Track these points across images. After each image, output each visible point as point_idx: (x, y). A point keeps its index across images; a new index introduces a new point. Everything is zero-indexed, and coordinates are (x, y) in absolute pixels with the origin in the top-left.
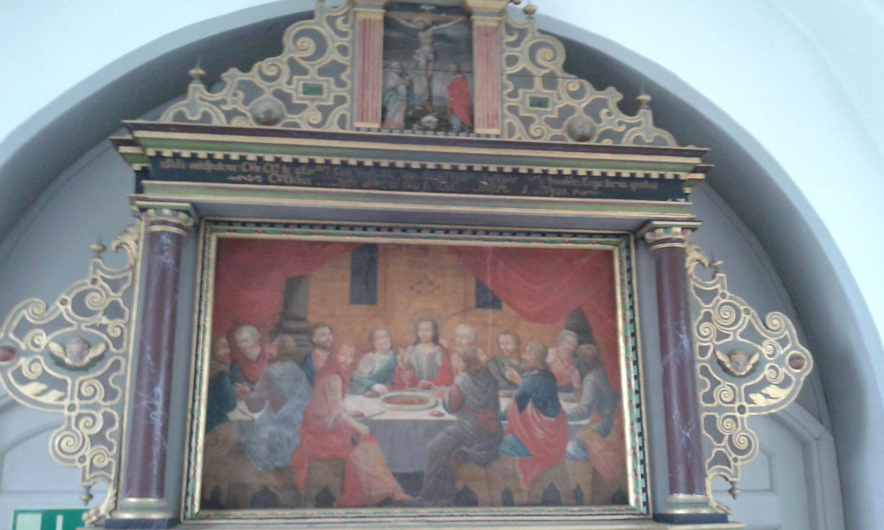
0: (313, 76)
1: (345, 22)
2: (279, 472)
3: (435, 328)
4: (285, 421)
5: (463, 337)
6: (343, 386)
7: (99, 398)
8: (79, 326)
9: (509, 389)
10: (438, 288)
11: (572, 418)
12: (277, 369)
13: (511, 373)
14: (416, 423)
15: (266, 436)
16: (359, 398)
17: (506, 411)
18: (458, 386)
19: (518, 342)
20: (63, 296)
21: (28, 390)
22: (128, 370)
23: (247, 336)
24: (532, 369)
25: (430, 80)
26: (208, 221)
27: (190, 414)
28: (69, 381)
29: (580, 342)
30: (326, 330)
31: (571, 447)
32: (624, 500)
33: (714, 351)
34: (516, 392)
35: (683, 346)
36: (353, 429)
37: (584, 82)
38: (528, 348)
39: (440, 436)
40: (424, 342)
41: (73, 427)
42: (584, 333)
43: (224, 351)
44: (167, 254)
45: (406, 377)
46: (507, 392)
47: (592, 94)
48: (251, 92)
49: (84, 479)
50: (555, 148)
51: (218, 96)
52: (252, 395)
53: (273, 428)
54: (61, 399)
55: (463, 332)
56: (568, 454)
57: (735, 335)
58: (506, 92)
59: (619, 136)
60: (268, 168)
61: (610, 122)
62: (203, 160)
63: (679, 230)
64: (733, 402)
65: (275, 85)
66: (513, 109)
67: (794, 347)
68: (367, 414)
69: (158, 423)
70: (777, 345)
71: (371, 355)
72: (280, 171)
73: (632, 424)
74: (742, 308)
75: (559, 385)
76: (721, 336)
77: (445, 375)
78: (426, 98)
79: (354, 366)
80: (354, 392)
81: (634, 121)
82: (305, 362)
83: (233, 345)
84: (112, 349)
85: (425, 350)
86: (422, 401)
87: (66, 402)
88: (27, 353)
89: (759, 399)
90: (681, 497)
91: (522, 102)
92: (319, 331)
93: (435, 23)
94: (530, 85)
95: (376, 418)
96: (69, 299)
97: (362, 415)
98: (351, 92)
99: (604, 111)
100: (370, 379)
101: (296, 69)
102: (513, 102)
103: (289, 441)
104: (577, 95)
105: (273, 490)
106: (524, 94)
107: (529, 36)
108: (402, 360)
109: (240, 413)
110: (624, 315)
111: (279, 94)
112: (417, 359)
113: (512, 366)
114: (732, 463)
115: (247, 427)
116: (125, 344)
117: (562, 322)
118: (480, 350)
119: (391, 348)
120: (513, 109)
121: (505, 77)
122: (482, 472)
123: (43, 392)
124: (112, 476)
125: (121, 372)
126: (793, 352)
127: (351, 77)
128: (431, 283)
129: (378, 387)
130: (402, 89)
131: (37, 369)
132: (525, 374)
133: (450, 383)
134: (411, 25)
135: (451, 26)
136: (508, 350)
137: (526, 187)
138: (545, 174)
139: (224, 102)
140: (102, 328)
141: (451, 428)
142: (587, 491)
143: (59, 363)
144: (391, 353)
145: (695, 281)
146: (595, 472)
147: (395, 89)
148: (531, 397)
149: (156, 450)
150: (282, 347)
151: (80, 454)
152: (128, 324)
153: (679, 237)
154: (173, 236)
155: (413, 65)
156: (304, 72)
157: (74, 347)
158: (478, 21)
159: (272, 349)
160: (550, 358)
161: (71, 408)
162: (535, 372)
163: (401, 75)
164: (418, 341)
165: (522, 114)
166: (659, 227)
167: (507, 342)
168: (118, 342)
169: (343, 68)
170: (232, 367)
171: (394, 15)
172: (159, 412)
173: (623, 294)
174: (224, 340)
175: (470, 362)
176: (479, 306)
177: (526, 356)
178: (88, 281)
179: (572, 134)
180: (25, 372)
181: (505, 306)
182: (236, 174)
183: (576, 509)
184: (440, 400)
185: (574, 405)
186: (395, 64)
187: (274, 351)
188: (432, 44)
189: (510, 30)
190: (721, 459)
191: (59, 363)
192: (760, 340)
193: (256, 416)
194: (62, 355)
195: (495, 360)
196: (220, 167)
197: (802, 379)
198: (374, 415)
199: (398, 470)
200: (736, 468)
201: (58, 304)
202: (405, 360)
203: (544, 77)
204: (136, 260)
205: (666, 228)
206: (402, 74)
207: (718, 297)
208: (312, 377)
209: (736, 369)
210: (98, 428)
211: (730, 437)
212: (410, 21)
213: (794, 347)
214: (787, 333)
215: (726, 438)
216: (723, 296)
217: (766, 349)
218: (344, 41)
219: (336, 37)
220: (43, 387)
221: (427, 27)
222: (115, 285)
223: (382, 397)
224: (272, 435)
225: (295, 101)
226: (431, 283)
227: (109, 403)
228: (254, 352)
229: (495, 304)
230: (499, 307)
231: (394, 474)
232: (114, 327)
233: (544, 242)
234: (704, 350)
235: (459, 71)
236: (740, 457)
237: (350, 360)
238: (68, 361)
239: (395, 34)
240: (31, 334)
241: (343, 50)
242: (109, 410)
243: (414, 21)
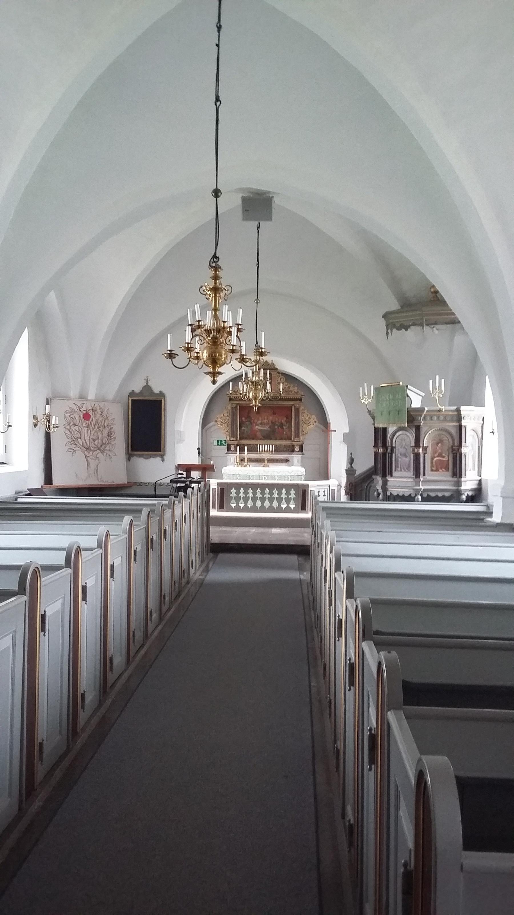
12: (247, 423)
13: (277, 423)
22: (230, 423)
42: (287, 418)
55: (271, 418)
57: (307, 418)
59: (292, 391)
76: (305, 418)
77: (268, 424)
82: (250, 422)
83: (242, 419)
85: (266, 420)
89: (309, 427)
104: (287, 385)
109: (243, 428)
115: (244, 430)
129: (260, 425)
142: (286, 438)
143: (222, 422)
157: (224, 421)
158: (273, 375)
160: (283, 421)
167: (277, 419)
168: (228, 420)
175: (271, 422)
179: (285, 391)
190: (304, 434)
191: (222, 422)
192: (310, 419)
195: (275, 421)
208: (251, 423)
222: (227, 413)
228: (244, 421)
232: (228, 418)
234: (302, 420)
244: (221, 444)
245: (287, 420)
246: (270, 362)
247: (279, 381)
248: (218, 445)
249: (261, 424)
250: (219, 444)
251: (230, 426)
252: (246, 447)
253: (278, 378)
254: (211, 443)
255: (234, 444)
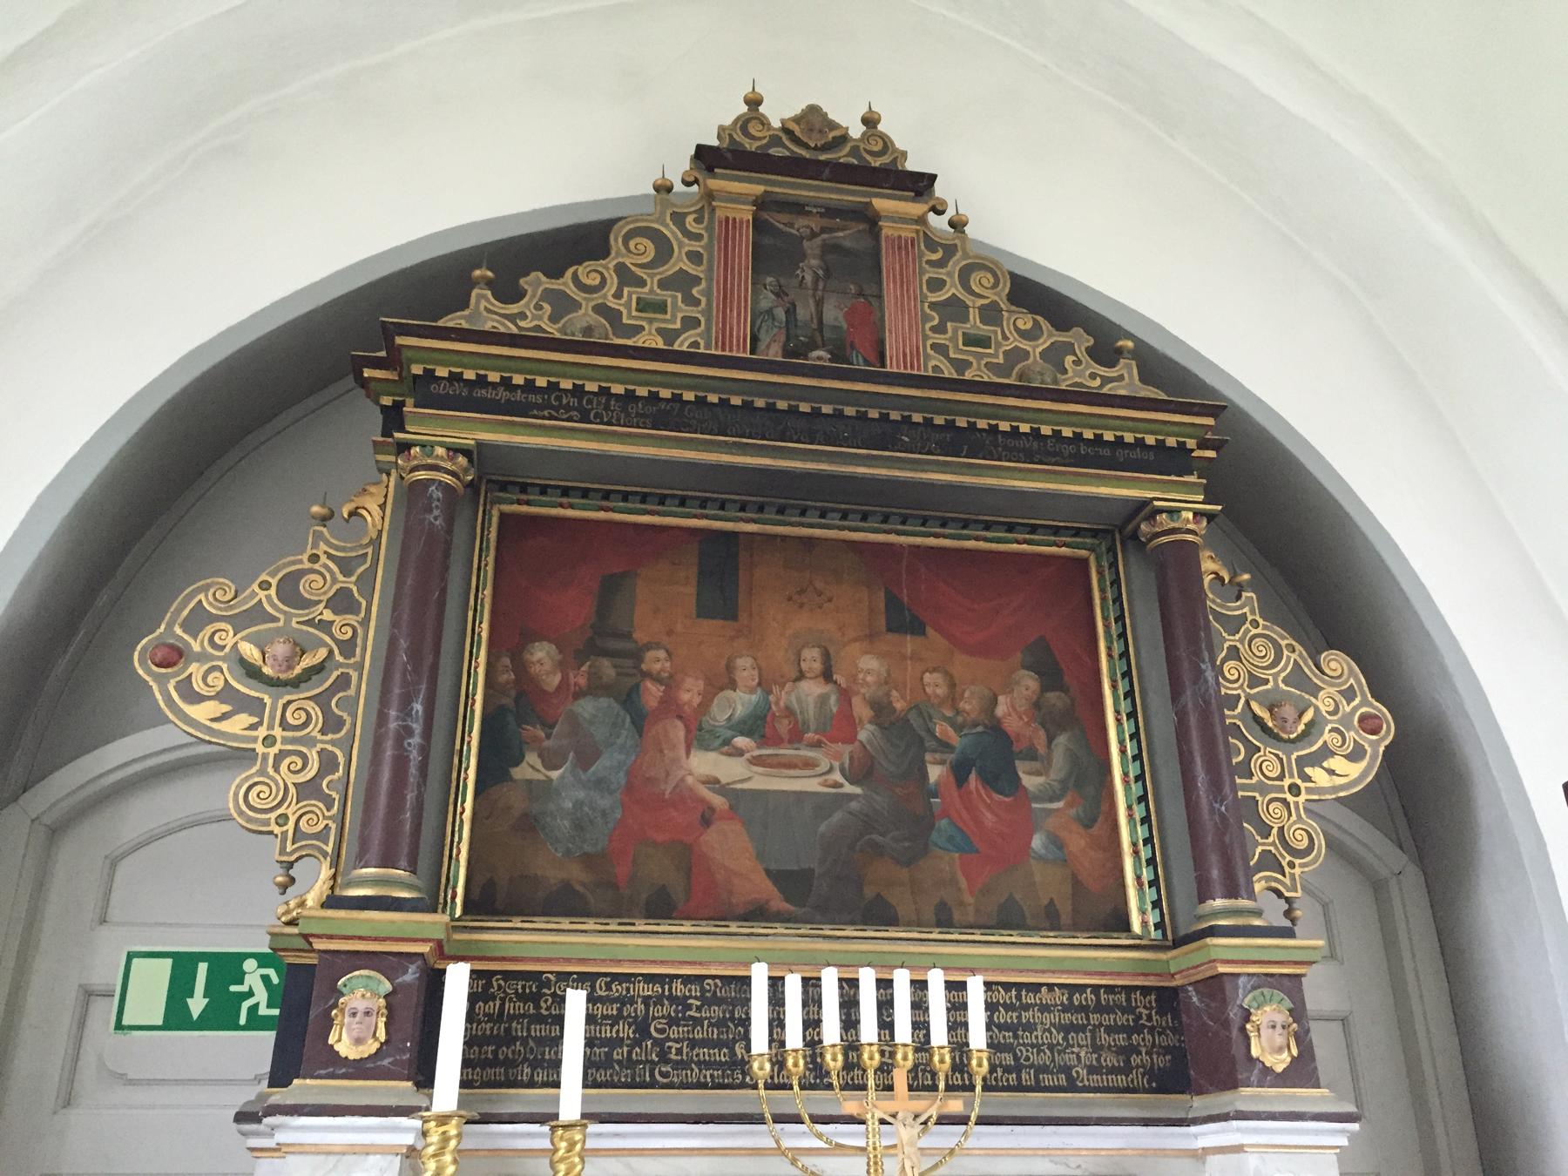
0: (651, 288)
1: (698, 221)
2: (588, 860)
3: (827, 657)
4: (600, 784)
5: (868, 672)
6: (686, 737)
7: (314, 730)
8: (288, 621)
9: (942, 752)
10: (830, 600)
11: (1038, 799)
12: (586, 708)
13: (941, 729)
14: (800, 796)
15: (568, 805)
16: (712, 755)
17: (937, 784)
18: (861, 742)
19: (952, 685)
20: (264, 577)
21: (201, 712)
22: (363, 689)
23: (542, 655)
24: (975, 725)
25: (819, 304)
26: (489, 481)
27: (452, 754)
28: (267, 700)
29: (1045, 689)
30: (662, 654)
31: (1037, 842)
32: (1126, 927)
33: (1247, 703)
34: (950, 757)
35: (1206, 681)
36: (703, 801)
37: (1038, 318)
38: (967, 694)
39: (837, 816)
40: (811, 678)
41: (271, 771)
42: (1050, 677)
43: (506, 677)
44: (436, 512)
45: (783, 727)
46: (938, 756)
47: (1050, 335)
48: (562, 305)
49: (283, 851)
50: (1008, 392)
51: (513, 309)
52: (547, 743)
53: (581, 794)
54: (253, 727)
55: (870, 665)
56: (1035, 853)
57: (1277, 679)
58: (928, 326)
60: (590, 402)
61: (1077, 374)
62: (494, 385)
63: (1190, 515)
64: (1281, 777)
65: (597, 298)
66: (940, 349)
67: (1364, 703)
68: (724, 781)
69: (414, 756)
70: (1338, 697)
71: (728, 693)
72: (607, 408)
73: (1129, 808)
74: (1283, 643)
75: (1016, 748)
77: (840, 727)
78: (815, 326)
79: (704, 706)
80: (707, 748)
81: (1115, 375)
82: (629, 699)
83: (520, 668)
84: (339, 658)
85: (812, 690)
86: (809, 764)
87: (262, 732)
88: (202, 657)
89: (1318, 775)
90: (1219, 903)
91: (954, 339)
92: (650, 655)
93: (823, 230)
94: (965, 319)
95: (739, 786)
96: (274, 582)
97: (717, 781)
98: (707, 312)
99: (1069, 359)
100: (730, 728)
101: (626, 276)
102: (940, 339)
103: (604, 814)
105: (578, 888)
106: (955, 330)
107: (959, 254)
108: (777, 704)
109: (529, 769)
110: (1109, 649)
111: (601, 309)
112: (799, 701)
113: (946, 719)
114: (1287, 869)
115: (540, 791)
116: (358, 650)
117: (1018, 657)
118: (894, 693)
119: (759, 684)
120: (940, 349)
121: (926, 304)
122: (904, 874)
123: (224, 717)
124: (329, 849)
125: (352, 692)
126: (1363, 710)
127: (708, 293)
128: (820, 594)
129: (741, 741)
130: (780, 313)
131: (217, 681)
132: (965, 731)
133: (851, 739)
134: (794, 232)
135: (847, 235)
136: (937, 696)
137: (966, 447)
138: (994, 429)
139: (523, 316)
140: (325, 626)
141: (854, 805)
142: (1065, 909)
143: (252, 672)
144: (759, 691)
145: (1213, 601)
146: (1076, 882)
147: (770, 312)
148: (974, 765)
149: (410, 796)
150: (593, 676)
151: (280, 811)
152: (365, 622)
153: (1191, 526)
154: (446, 488)
155: (795, 282)
156: (641, 283)
157: (280, 649)
158: (888, 229)
159: (580, 679)
160: (1001, 710)
161: (269, 741)
162: (980, 729)
163: (777, 295)
164: (801, 676)
165: (952, 355)
166: (1161, 511)
167: (935, 684)
168: (348, 647)
169: (696, 280)
170: (517, 700)
171: (765, 215)
172: (416, 740)
173: (1105, 618)
174: (506, 661)
175: (880, 709)
176: (889, 630)
177: (964, 705)
178: (305, 557)
180: (198, 685)
181: (930, 631)
182: (541, 407)
183: (1052, 934)
184: (836, 764)
185: (1040, 780)
186: (769, 279)
187: (582, 681)
188: (822, 257)
189: (932, 245)
190: (1270, 862)
191: (252, 672)
192: (1315, 691)
193: (555, 774)
194: (260, 662)
196: (519, 396)
197: (1382, 749)
198: (735, 782)
199: (773, 866)
200: (1293, 876)
201: (255, 587)
202: (782, 704)
203: (982, 309)
204: (380, 532)
205: (1172, 512)
206: (780, 293)
207: (1248, 625)
208: (640, 721)
209: (1283, 729)
210: (310, 773)
211: (1281, 829)
212: (791, 225)
213: (1364, 703)
214: (1352, 681)
215: (1275, 831)
216: (1255, 624)
217: (1324, 703)
218: (696, 246)
219: (686, 241)
220: (226, 708)
221: (814, 235)
222: (346, 566)
223: (747, 756)
224: (578, 804)
225: (625, 321)
226: (820, 594)
227: (330, 737)
229: (916, 628)
230: (924, 633)
231: (768, 872)
232: (343, 627)
233: (986, 539)
235: (860, 294)
236: (1297, 862)
237: (697, 700)
238: (267, 670)
239: (768, 241)
240: (209, 630)
241: (695, 257)
242: (330, 747)
243: (796, 226)
244: (222, 1014)
245: (1053, 697)
246: (856, 131)
247: (952, 289)
248: (177, 1017)
249: (758, 725)
250: (197, 1004)
251: (359, 722)
252: (576, 1002)
253: (941, 264)
254: (89, 995)
255: (385, 963)
